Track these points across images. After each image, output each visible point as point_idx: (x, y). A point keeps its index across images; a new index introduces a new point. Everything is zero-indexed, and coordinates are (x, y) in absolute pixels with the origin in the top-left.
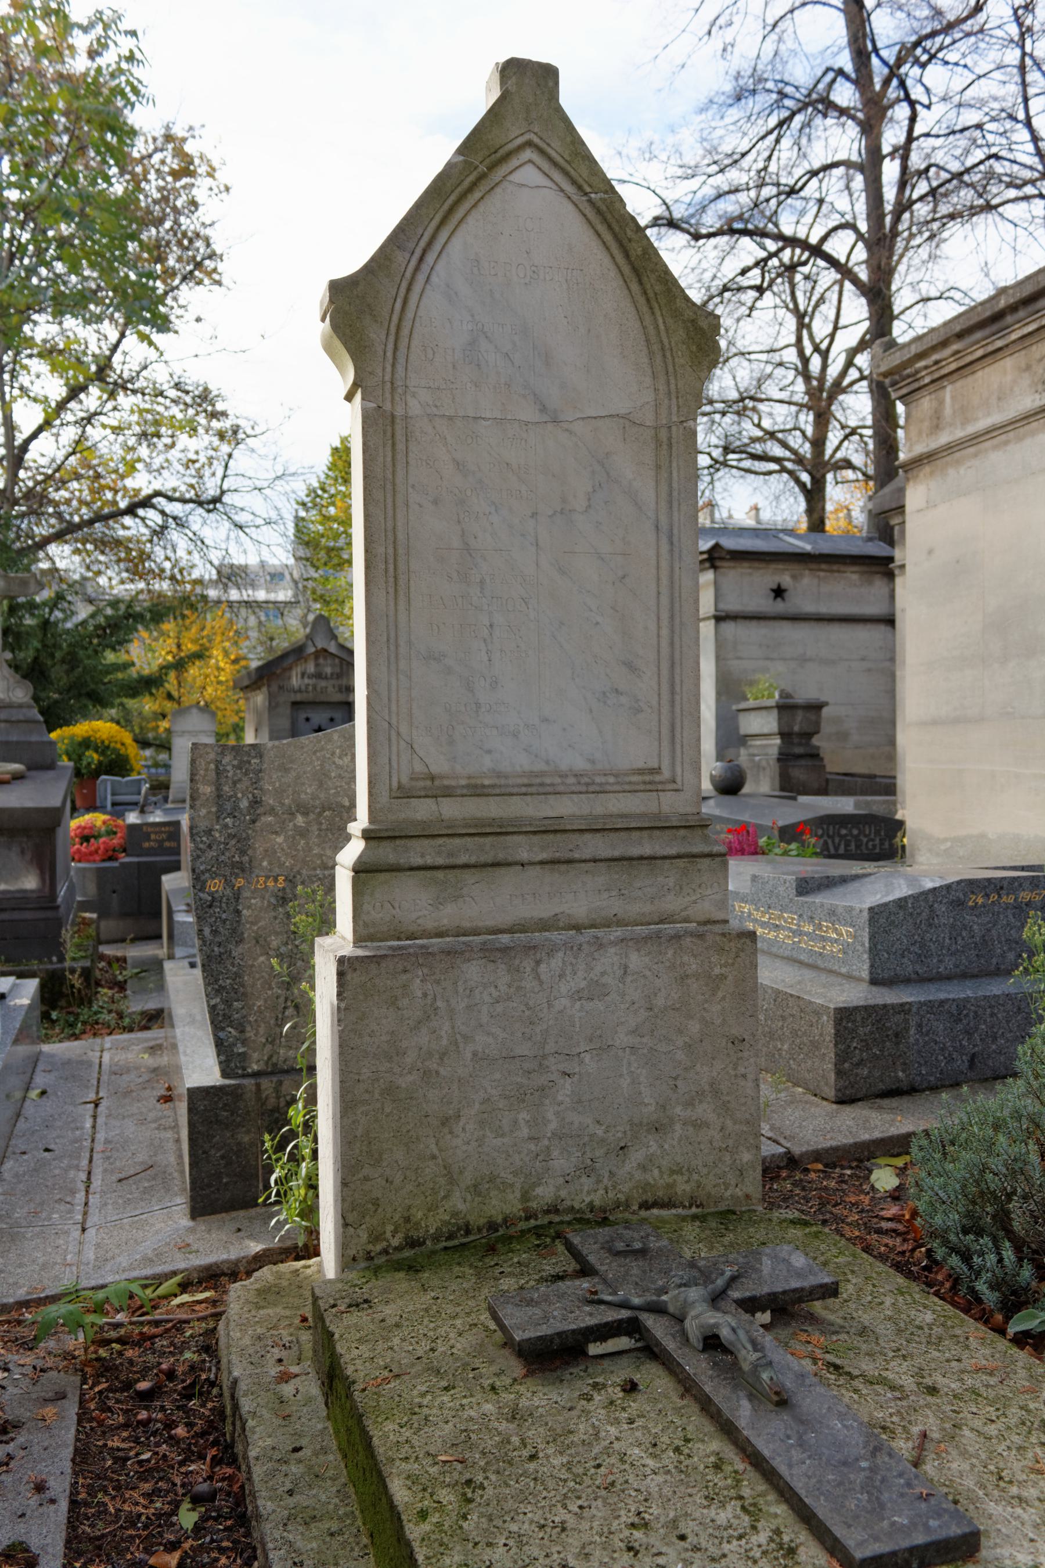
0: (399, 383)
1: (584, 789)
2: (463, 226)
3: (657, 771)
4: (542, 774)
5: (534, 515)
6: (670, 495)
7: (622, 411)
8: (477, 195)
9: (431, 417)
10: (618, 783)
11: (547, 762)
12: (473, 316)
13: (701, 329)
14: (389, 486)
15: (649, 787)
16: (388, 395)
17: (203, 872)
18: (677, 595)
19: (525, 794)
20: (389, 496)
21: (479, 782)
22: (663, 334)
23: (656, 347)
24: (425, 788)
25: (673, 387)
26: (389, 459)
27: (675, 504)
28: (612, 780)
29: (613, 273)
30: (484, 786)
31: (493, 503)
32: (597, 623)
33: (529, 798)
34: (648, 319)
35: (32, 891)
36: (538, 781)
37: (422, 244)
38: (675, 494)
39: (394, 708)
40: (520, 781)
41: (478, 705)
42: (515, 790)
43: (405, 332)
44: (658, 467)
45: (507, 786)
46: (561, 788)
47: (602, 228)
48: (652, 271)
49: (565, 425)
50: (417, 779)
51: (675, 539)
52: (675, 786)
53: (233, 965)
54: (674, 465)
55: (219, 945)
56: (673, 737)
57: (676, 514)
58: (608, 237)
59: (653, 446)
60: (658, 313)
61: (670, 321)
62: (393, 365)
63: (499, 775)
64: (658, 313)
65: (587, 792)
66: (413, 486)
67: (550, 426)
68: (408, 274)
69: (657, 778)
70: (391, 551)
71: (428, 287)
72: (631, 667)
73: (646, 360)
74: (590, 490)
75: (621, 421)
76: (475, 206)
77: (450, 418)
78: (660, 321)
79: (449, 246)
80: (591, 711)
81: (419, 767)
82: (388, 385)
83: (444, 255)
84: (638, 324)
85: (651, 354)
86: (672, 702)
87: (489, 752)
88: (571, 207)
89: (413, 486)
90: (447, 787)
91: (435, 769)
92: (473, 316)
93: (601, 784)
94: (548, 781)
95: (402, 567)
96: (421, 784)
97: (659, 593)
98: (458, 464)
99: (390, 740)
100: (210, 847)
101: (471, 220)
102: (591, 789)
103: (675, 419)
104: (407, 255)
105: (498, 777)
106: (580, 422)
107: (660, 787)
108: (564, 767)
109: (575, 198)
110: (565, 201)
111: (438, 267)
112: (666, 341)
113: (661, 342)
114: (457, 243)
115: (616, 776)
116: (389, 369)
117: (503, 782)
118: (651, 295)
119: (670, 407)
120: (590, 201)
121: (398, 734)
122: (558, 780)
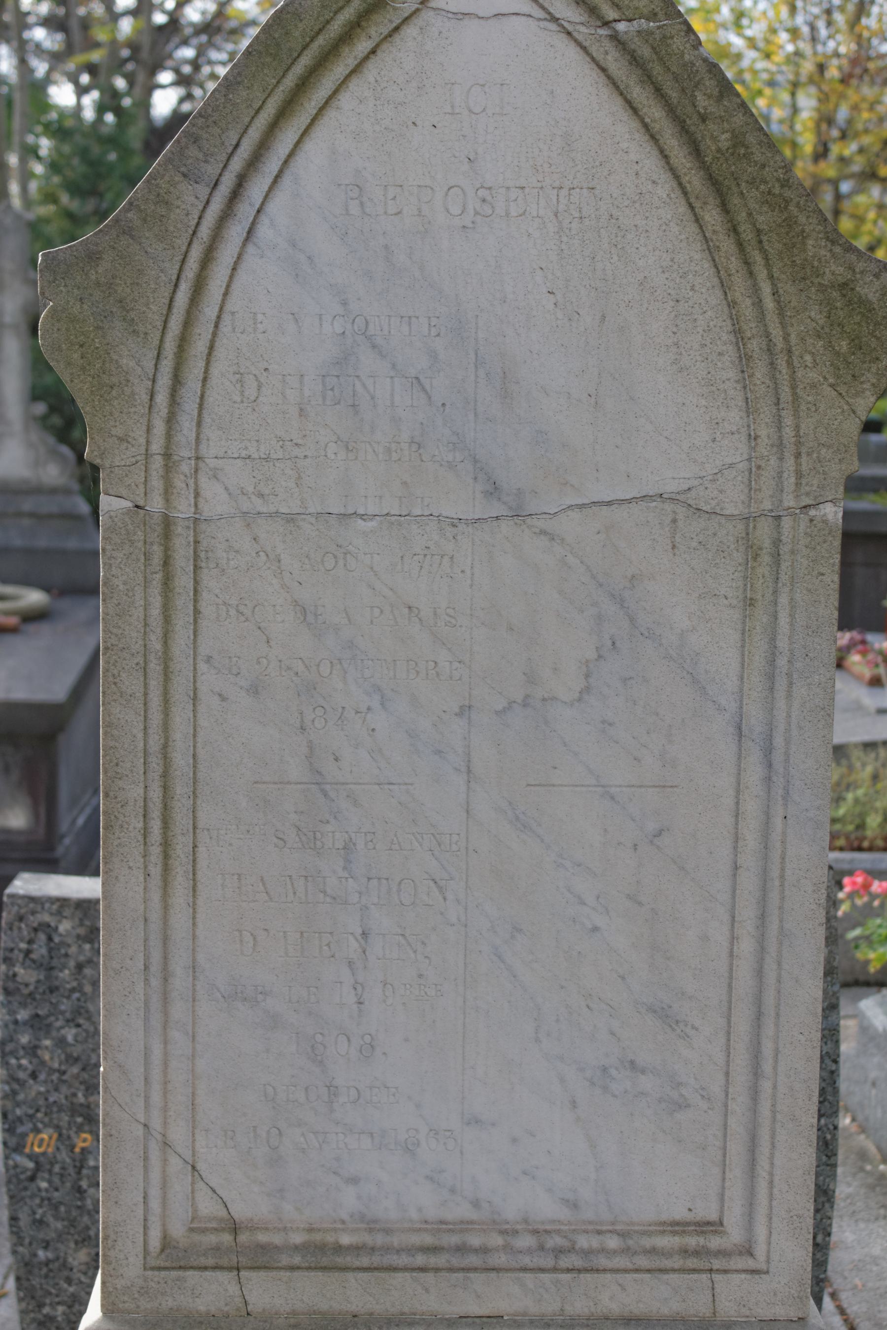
0: (184, 452)
1: (549, 1262)
2: (331, 114)
3: (714, 1226)
4: (465, 1226)
5: (464, 710)
6: (772, 662)
7: (671, 487)
8: (362, 46)
9: (249, 518)
10: (626, 1251)
11: (476, 1204)
12: (344, 303)
13: (863, 302)
14: (155, 667)
15: (692, 1263)
16: (157, 483)
17: (20, 1120)
18: (775, 873)
19: (423, 1270)
20: (155, 685)
21: (330, 1238)
22: (772, 318)
23: (755, 346)
24: (217, 1249)
25: (788, 432)
26: (156, 611)
27: (781, 684)
28: (613, 1243)
29: (665, 188)
30: (339, 1249)
31: (378, 689)
32: (595, 929)
33: (430, 1277)
34: (740, 283)
35: (19, 832)
36: (455, 1239)
37: (237, 165)
38: (782, 662)
39: (156, 1097)
40: (415, 1239)
41: (333, 1090)
42: (404, 1260)
43: (199, 346)
44: (750, 603)
45: (387, 1249)
46: (501, 1259)
47: (639, 94)
48: (752, 182)
49: (540, 523)
50: (204, 1231)
51: (778, 757)
52: (751, 1264)
53: (69, 1281)
54: (783, 600)
55: (46, 1246)
56: (753, 1163)
57: (781, 704)
58: (655, 113)
59: (739, 557)
60: (762, 274)
61: (787, 288)
62: (171, 419)
63: (372, 1225)
64: (762, 274)
65: (555, 1270)
66: (209, 659)
67: (505, 527)
68: (205, 231)
69: (715, 1242)
70: (156, 794)
71: (251, 249)
72: (663, 1014)
73: (732, 374)
74: (591, 654)
75: (669, 507)
76: (356, 70)
77: (291, 519)
78: (766, 289)
79: (300, 160)
80: (574, 1104)
81: (207, 1207)
82: (157, 463)
83: (287, 181)
84: (716, 297)
85: (745, 359)
86: (755, 1094)
87: (354, 1181)
88: (572, 52)
89: (209, 659)
90: (264, 1248)
91: (239, 1211)
92: (344, 303)
93: (587, 1253)
94: (475, 1241)
95: (181, 819)
96: (212, 1239)
97: (736, 867)
98: (302, 610)
99: (146, 1159)
100: (34, 1075)
101: (345, 100)
102: (565, 1262)
103: (789, 501)
104: (203, 191)
105: (371, 1230)
106: (575, 515)
107: (717, 1264)
108: (511, 1212)
109: (582, 32)
110: (561, 42)
111: (272, 207)
112: (776, 332)
113: (768, 335)
114: (315, 151)
115: (623, 1235)
116: (159, 427)
117: (380, 1239)
118: (747, 234)
119: (780, 474)
120: (615, 37)
121: (166, 1144)
122: (497, 1240)
